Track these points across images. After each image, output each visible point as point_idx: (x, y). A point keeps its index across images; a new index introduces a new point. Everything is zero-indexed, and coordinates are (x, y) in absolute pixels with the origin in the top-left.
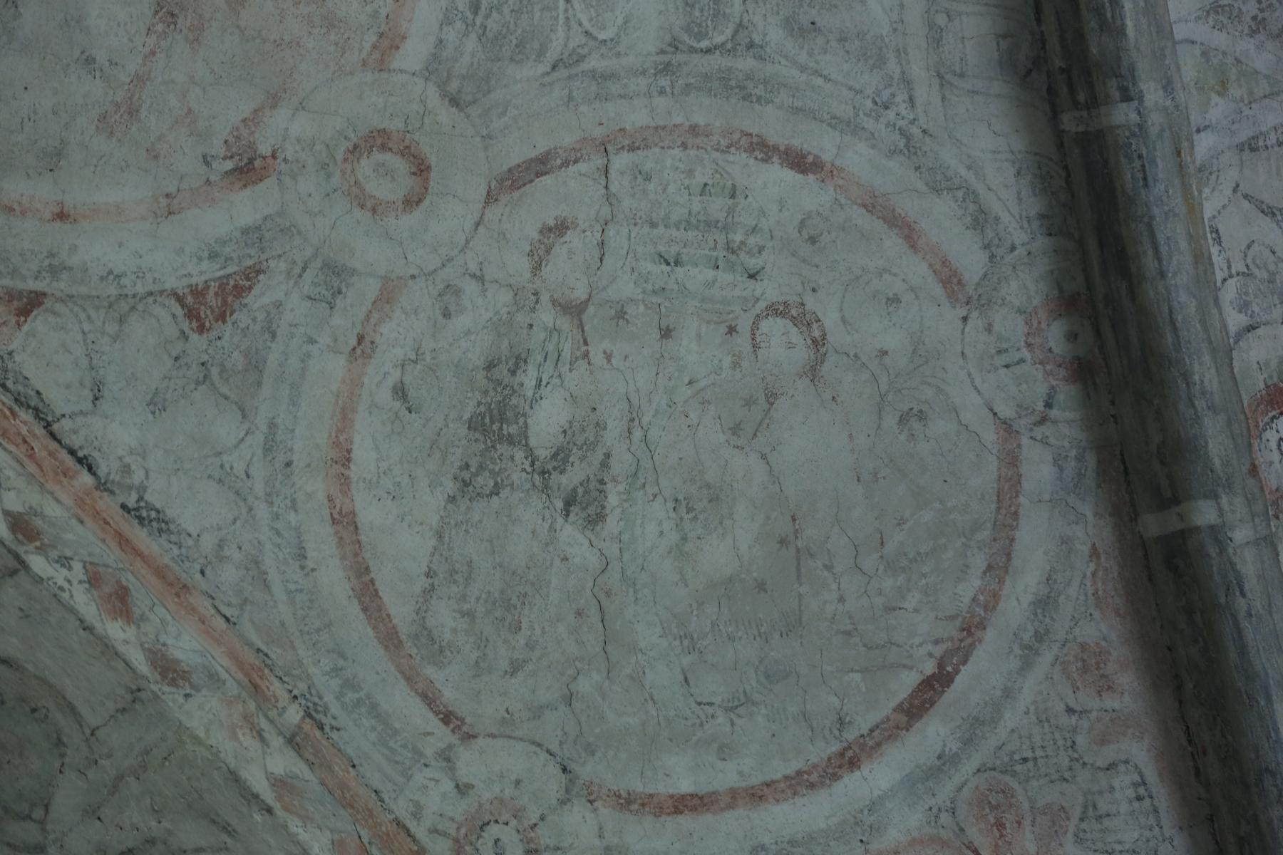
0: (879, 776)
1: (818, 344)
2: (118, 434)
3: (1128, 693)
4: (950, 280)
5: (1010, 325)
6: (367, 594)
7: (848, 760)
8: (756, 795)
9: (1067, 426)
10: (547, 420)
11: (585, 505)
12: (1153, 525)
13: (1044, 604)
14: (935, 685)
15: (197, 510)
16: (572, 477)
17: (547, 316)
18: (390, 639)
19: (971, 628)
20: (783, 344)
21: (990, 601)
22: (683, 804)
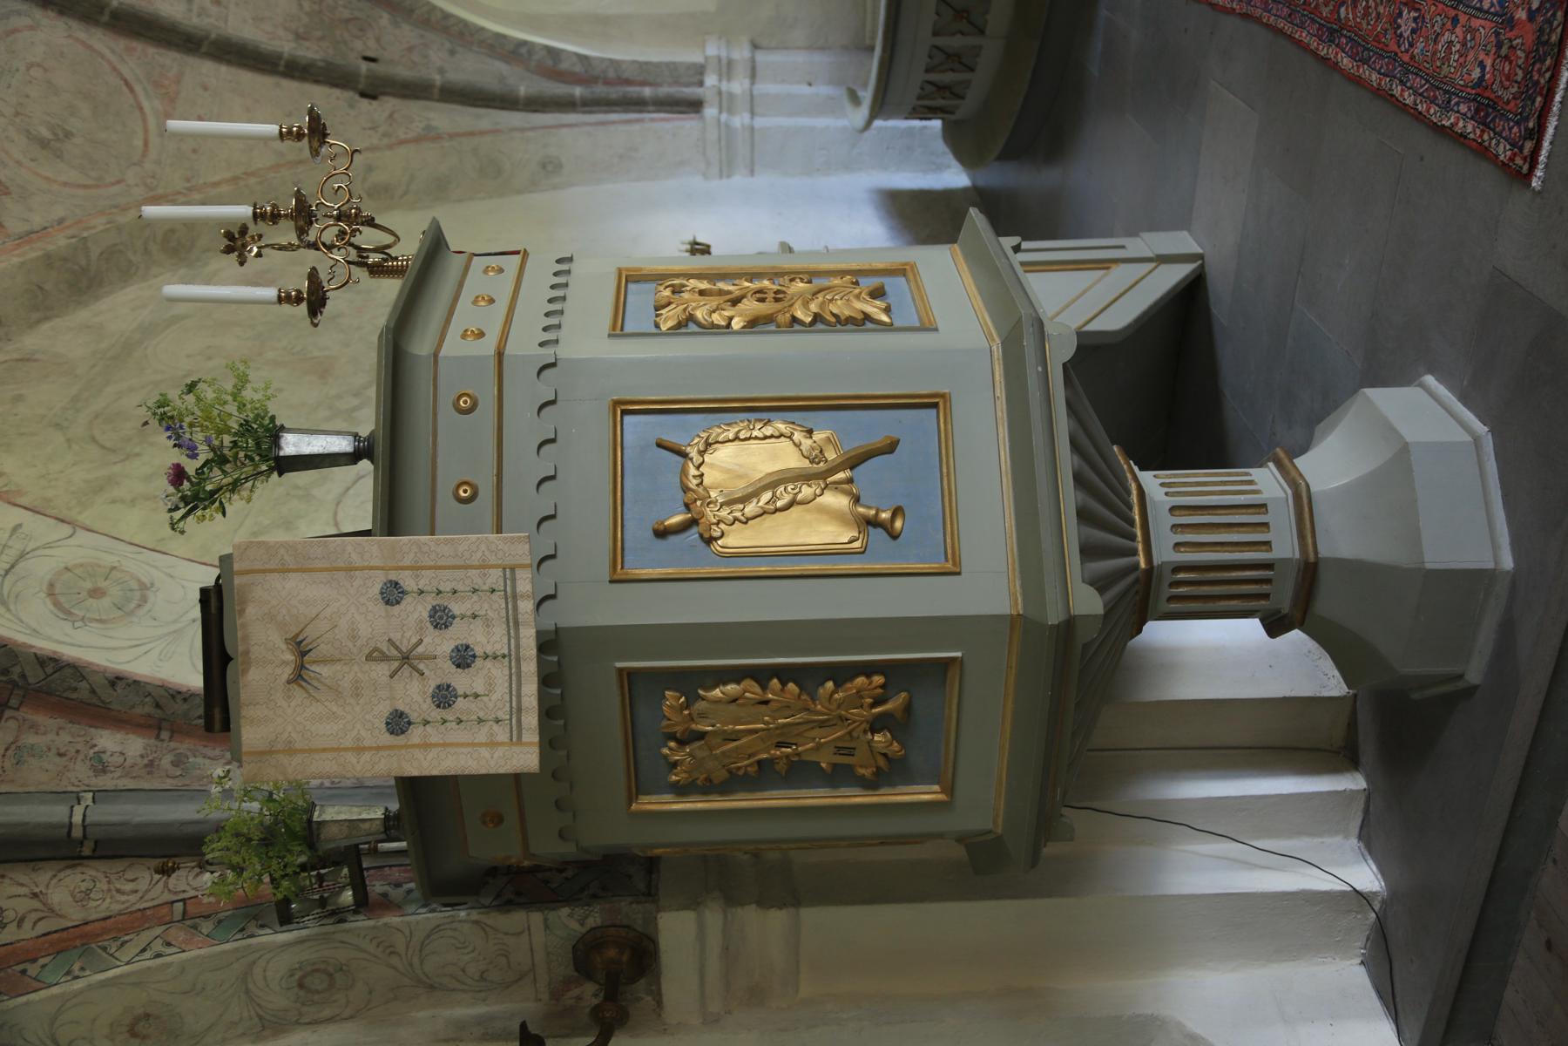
0: (146, 105)
1: (39, 65)
2: (37, 220)
3: (138, 46)
4: (31, 28)
5: (45, 22)
6: (85, 187)
7: (141, 109)
8: (146, 131)
9: (74, 24)
10: (45, 133)
11: (68, 135)
12: (105, 18)
13: (113, 51)
14: (127, 83)
15: (59, 211)
16: (61, 135)
17: (17, 120)
18: (98, 186)
19: (114, 69)
20: (35, 72)
21: (109, 62)
22: (146, 143)
